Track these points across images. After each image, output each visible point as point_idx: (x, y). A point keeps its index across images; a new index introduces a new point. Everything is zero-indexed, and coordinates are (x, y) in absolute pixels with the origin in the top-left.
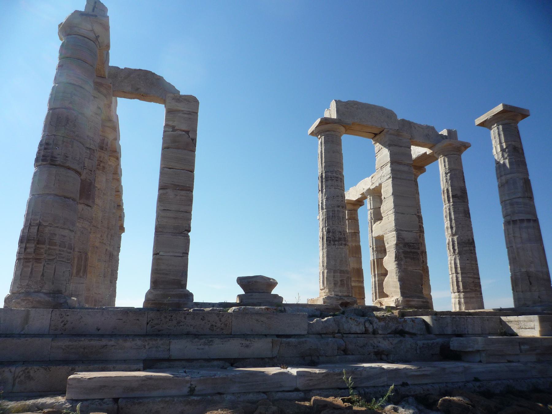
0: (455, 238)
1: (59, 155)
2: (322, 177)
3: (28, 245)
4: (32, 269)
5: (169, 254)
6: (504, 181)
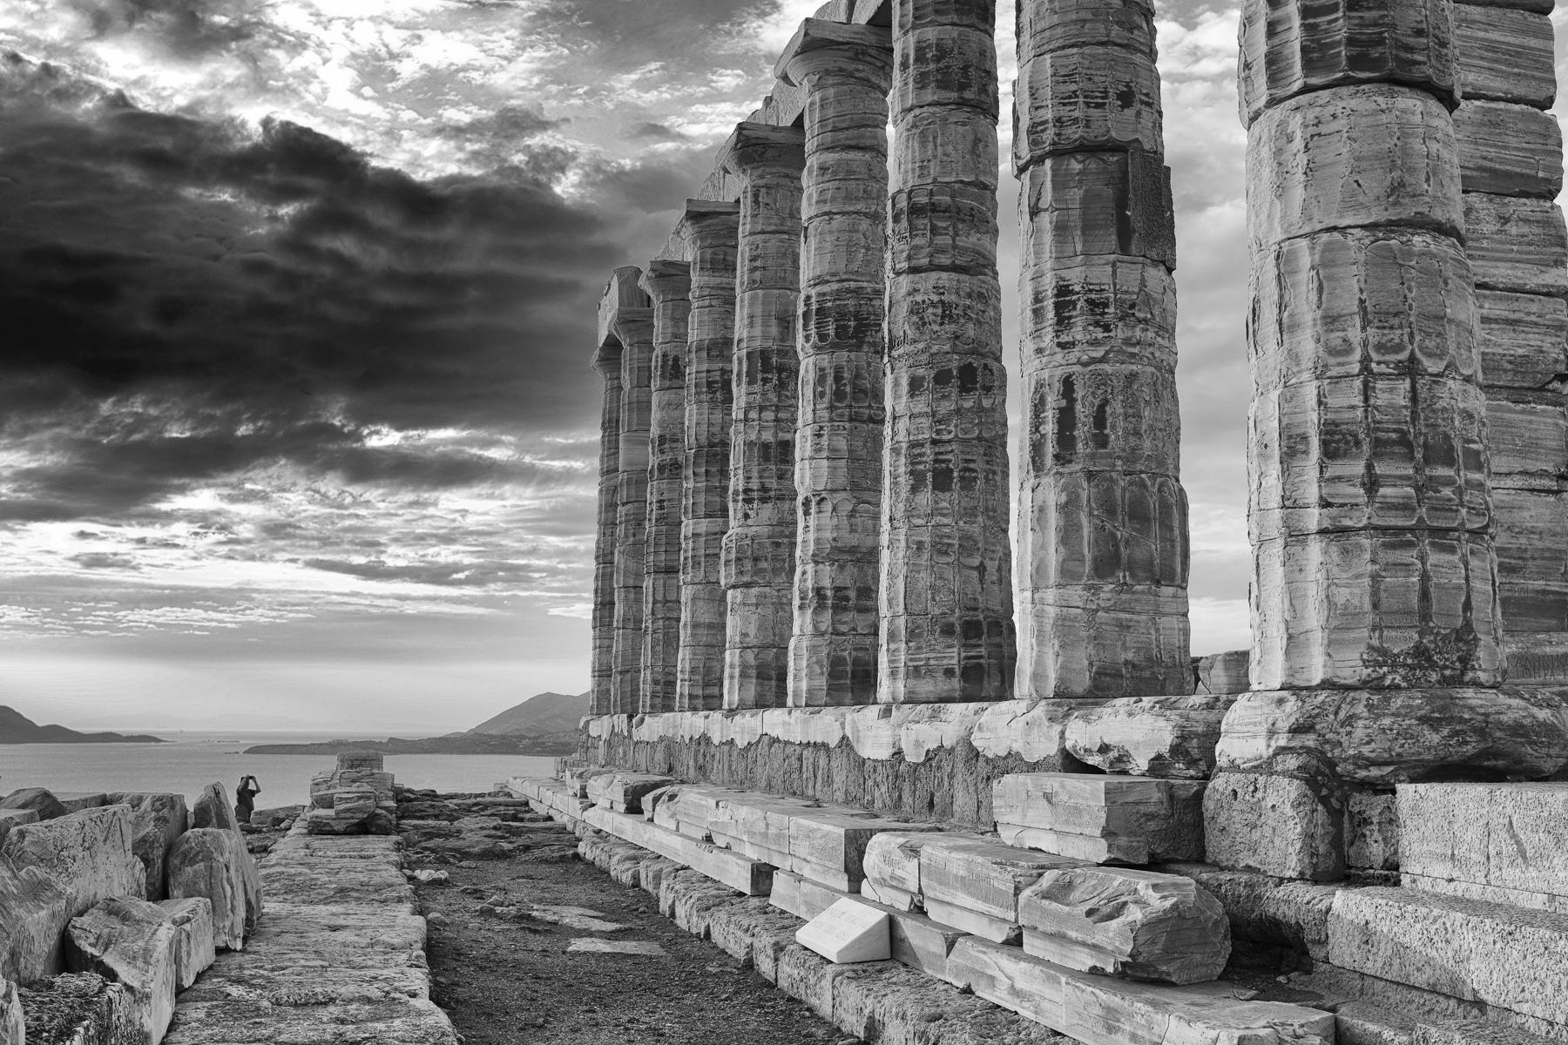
1: (1419, 33)
3: (1379, 469)
4: (1425, 577)
5: (1509, 483)
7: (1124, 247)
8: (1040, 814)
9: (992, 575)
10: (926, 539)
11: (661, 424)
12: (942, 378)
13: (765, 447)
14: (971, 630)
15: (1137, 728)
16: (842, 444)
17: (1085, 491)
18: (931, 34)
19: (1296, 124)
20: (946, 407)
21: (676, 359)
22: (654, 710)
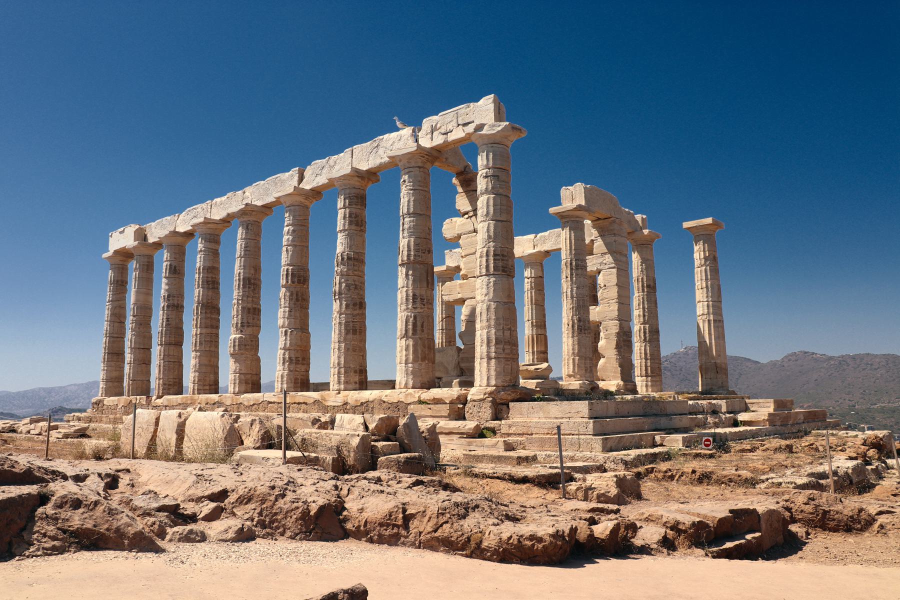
10: (351, 348)
13: (249, 309)
16: (298, 315)
17: (419, 342)
18: (354, 210)
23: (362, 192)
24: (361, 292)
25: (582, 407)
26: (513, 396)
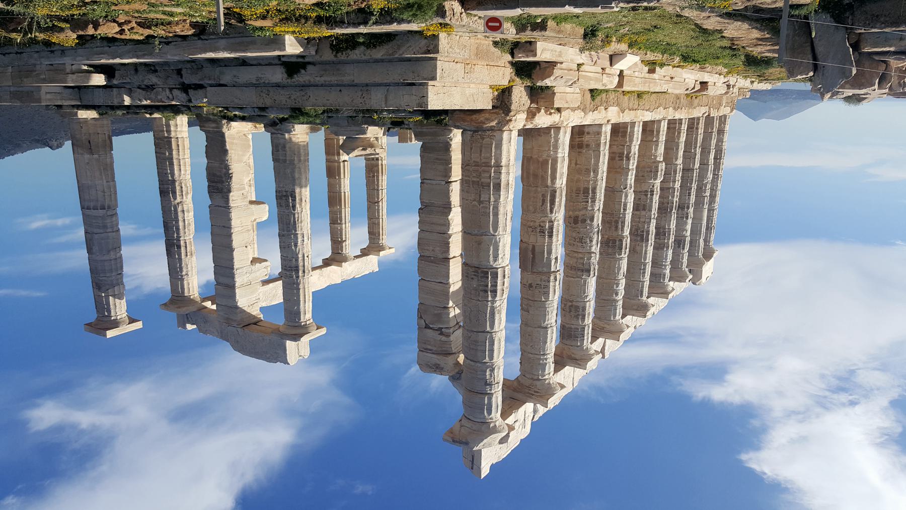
0: (179, 199)
2: (304, 272)
6: (112, 253)
7: (534, 247)
8: (569, 97)
9: (573, 162)
11: (686, 223)
12: (584, 221)
13: (644, 210)
14: (580, 146)
15: (543, 120)
16: (617, 206)
19: (500, 261)
20: (582, 213)
21: (679, 247)
22: (698, 119)
23: (568, 342)
24: (574, 235)
25: (435, 102)
26: (481, 117)
